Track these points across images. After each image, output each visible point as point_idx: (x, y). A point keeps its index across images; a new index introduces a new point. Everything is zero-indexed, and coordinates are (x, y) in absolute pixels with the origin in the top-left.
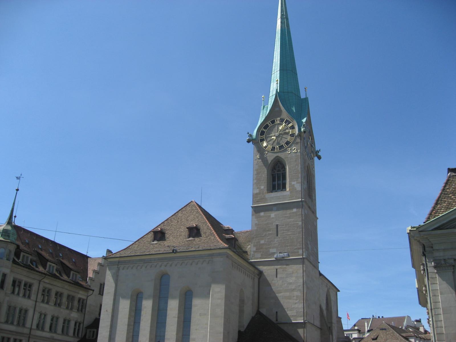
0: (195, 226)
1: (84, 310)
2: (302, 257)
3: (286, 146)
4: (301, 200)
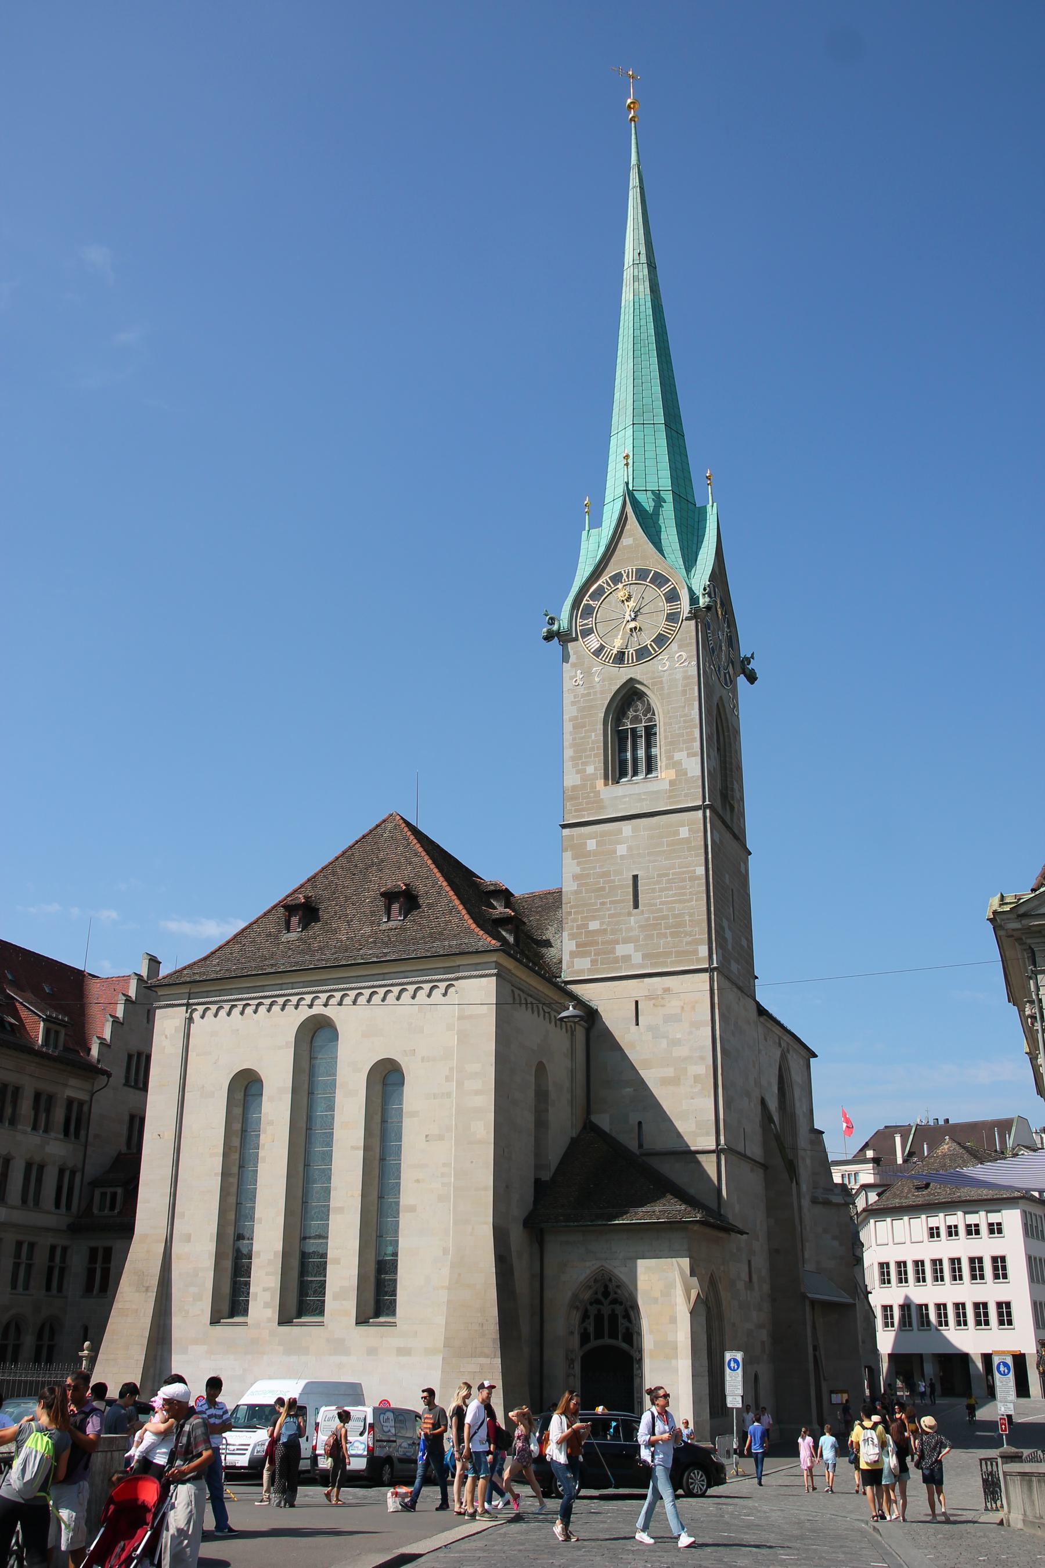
0: (404, 887)
1: (83, 1133)
2: (707, 966)
4: (701, 803)
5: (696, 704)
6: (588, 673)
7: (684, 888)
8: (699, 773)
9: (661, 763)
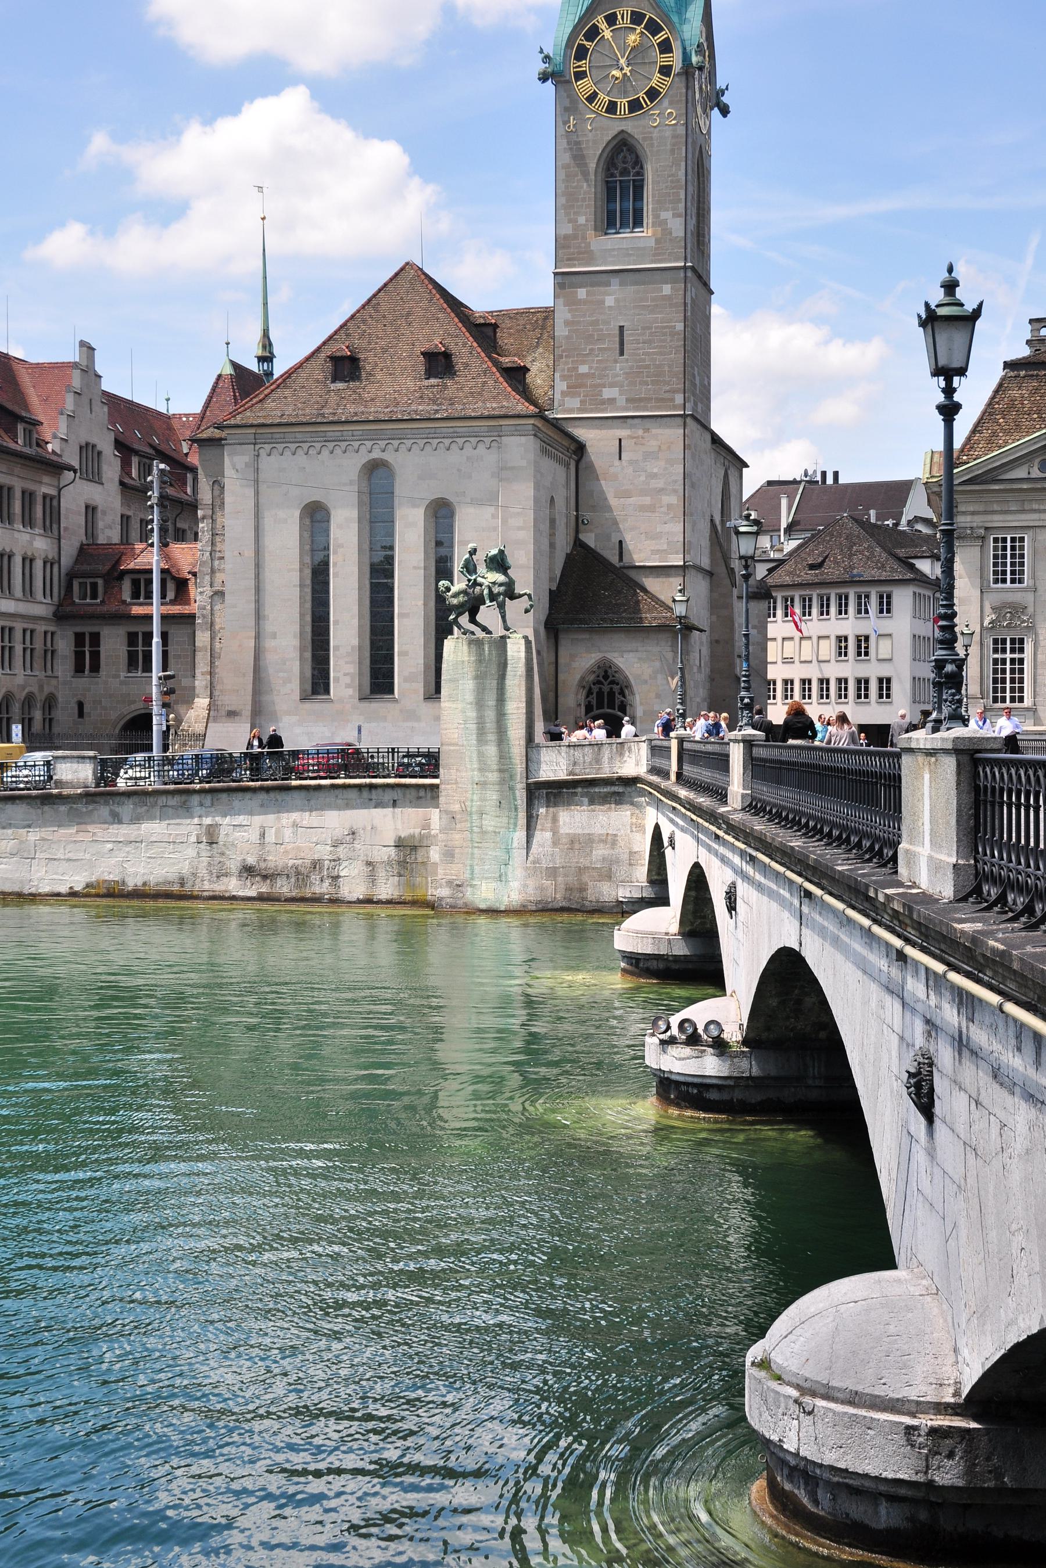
1: (55, 526)
7: (664, 341)
9: (648, 218)
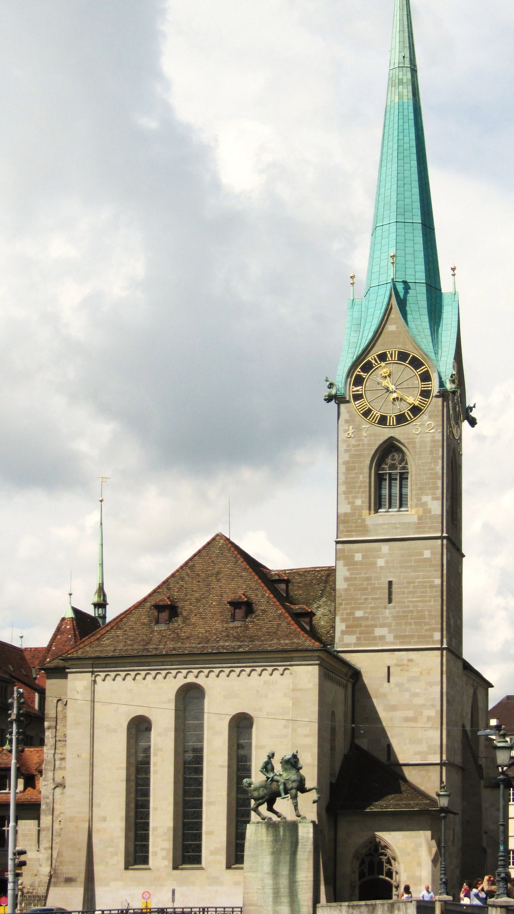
3: (412, 417)
5: (440, 461)
6: (358, 429)
8: (439, 512)
